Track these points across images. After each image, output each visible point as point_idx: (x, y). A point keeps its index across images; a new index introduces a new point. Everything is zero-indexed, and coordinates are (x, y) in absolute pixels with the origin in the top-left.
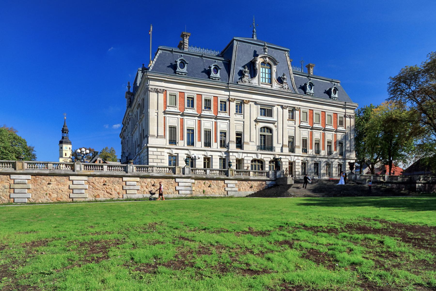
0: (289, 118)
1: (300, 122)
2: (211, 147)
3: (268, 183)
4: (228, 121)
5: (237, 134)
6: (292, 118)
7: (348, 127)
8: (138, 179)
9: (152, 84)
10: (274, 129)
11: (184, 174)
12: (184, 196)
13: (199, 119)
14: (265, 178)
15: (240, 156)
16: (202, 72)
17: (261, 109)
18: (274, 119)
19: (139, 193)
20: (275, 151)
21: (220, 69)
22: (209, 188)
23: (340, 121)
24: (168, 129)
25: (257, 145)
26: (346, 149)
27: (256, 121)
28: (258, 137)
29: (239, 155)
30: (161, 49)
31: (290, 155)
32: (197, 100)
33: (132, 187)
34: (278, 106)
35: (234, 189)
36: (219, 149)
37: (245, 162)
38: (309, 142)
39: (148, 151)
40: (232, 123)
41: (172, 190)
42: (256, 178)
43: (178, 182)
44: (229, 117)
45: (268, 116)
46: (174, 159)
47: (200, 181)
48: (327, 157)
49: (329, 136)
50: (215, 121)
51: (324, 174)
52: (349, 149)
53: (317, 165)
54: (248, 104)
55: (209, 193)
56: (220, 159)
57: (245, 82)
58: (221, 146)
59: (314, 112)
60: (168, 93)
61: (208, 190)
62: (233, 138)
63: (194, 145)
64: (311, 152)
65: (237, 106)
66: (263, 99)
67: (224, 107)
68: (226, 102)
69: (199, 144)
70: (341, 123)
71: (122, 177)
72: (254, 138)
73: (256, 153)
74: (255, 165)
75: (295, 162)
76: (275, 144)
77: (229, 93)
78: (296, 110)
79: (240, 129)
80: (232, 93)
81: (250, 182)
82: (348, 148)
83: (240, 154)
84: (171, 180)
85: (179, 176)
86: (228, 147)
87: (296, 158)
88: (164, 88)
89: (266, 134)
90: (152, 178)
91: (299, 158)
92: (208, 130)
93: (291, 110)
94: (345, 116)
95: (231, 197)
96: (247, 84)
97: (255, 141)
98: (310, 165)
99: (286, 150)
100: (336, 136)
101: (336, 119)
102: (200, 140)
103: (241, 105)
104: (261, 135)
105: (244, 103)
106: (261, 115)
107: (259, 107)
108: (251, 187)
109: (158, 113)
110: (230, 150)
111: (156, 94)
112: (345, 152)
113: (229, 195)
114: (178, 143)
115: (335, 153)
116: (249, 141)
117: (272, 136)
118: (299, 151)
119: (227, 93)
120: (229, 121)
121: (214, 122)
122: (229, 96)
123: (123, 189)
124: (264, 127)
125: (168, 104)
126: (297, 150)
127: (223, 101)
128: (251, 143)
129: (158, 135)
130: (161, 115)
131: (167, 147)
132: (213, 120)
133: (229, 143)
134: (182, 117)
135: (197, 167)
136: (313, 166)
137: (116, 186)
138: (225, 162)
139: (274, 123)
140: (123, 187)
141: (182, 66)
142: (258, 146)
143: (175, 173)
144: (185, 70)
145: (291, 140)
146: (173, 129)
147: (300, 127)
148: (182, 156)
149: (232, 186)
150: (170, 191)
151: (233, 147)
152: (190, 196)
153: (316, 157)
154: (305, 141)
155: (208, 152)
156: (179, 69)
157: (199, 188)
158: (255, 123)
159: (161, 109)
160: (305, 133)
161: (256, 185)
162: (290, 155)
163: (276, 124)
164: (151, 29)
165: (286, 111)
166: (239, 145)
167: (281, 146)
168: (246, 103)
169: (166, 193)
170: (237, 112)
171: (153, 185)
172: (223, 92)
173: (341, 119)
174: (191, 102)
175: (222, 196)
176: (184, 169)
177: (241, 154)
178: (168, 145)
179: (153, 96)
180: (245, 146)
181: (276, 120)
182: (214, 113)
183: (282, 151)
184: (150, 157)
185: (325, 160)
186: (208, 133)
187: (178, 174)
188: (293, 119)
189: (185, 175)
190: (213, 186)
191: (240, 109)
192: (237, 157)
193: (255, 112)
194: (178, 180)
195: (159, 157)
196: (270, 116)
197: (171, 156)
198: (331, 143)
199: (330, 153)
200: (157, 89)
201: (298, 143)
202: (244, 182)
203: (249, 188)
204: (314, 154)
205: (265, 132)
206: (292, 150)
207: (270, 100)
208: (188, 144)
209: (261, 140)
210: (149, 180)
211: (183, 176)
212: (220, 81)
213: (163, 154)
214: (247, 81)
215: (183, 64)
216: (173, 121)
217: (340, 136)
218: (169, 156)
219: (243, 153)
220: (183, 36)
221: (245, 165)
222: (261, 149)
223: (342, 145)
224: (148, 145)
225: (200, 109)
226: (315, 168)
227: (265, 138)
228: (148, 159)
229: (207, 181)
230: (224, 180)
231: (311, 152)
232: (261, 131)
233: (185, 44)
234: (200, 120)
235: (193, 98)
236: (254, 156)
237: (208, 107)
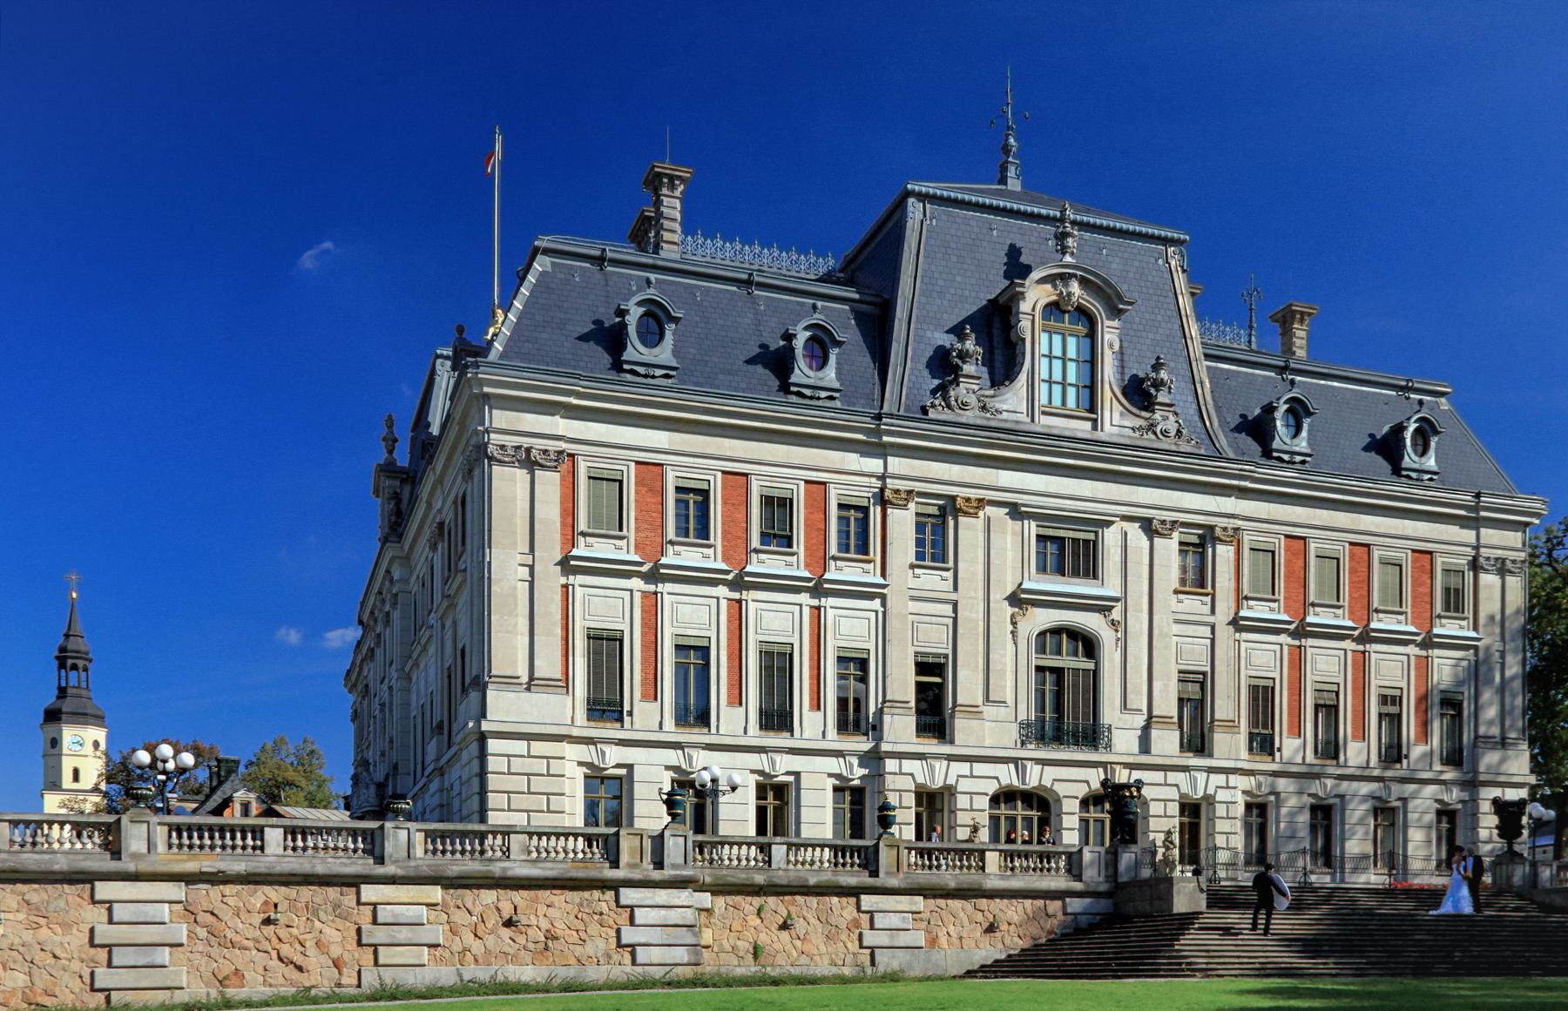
0: (1183, 582)
1: (1240, 599)
2: (791, 731)
3: (1075, 905)
4: (878, 601)
5: (923, 668)
6: (1198, 579)
7: (1492, 618)
8: (436, 893)
9: (506, 425)
10: (1107, 636)
11: (659, 864)
12: (657, 973)
13: (736, 596)
14: (1059, 882)
15: (940, 775)
16: (750, 362)
17: (1041, 538)
18: (1111, 588)
19: (439, 961)
20: (1109, 746)
21: (839, 344)
22: (785, 935)
23: (1447, 591)
24: (580, 644)
25: (1022, 716)
26: (1482, 730)
27: (1015, 599)
28: (1027, 680)
29: (932, 769)
30: (546, 252)
31: (1185, 769)
32: (724, 503)
33: (403, 934)
34: (1126, 525)
35: (904, 939)
36: (834, 740)
37: (962, 802)
38: (1282, 700)
39: (483, 755)
40: (896, 612)
41: (600, 943)
42: (1016, 883)
43: (632, 907)
44: (882, 581)
45: (1076, 573)
46: (610, 795)
47: (739, 898)
48: (1376, 773)
49: (1390, 669)
50: (815, 602)
51: (1365, 857)
52: (1495, 731)
53: (1324, 815)
54: (975, 516)
55: (781, 960)
56: (836, 789)
57: (964, 406)
58: (842, 726)
59: (1312, 546)
60: (582, 467)
61: (777, 946)
62: (904, 684)
63: (708, 725)
64: (1293, 748)
65: (920, 528)
66: (1052, 490)
67: (858, 533)
68: (865, 510)
69: (735, 719)
70: (1454, 602)
71: (354, 882)
72: (1005, 686)
73: (1015, 761)
74: (1012, 820)
75: (1210, 800)
76: (1110, 713)
77: (880, 462)
78: (1216, 540)
79: (936, 642)
80: (896, 464)
81: (983, 903)
82: (1490, 723)
83: (937, 764)
84: (596, 894)
85: (636, 875)
86: (876, 729)
87: (1219, 779)
88: (563, 445)
89: (1066, 662)
90: (505, 887)
91: (1234, 780)
92: (776, 649)
93: (1195, 540)
94: (1475, 565)
95: (893, 978)
96: (969, 416)
97: (1010, 700)
98: (1292, 815)
99: (1167, 743)
100: (1424, 665)
101: (1426, 578)
102: (738, 699)
103: (944, 523)
104: (1039, 669)
105: (957, 512)
106: (1042, 569)
107: (1032, 528)
108: (991, 929)
109: (532, 568)
110: (885, 747)
111: (521, 475)
112: (1475, 745)
113: (881, 969)
114: (630, 713)
115: (1417, 751)
116: (980, 700)
117: (1096, 673)
118: (1231, 746)
119: (875, 465)
120: (884, 604)
121: (806, 610)
122: (883, 478)
123: (360, 944)
124: (1057, 631)
125: (582, 526)
126: (1220, 740)
127: (854, 502)
128: (989, 711)
129: (531, 678)
130: (551, 579)
131: (575, 732)
132: (804, 598)
133: (880, 713)
134: (652, 588)
135: (725, 829)
136: (1304, 818)
137: (327, 930)
138: (861, 805)
139: (1104, 610)
140: (359, 931)
141: (652, 336)
142: (1024, 725)
143: (615, 864)
144: (664, 353)
145: (1193, 690)
146: (605, 646)
147: (1236, 623)
148: (652, 776)
149: (894, 921)
150: (590, 949)
151: (901, 729)
152: (688, 972)
153: (1317, 776)
154: (1262, 698)
155: (778, 757)
156: (636, 351)
157: (735, 933)
158: (1010, 610)
159: (550, 550)
160: (1265, 657)
161: (1016, 918)
162: (1185, 769)
163: (1116, 614)
164: (498, 147)
165: (1169, 548)
166: (928, 719)
167: (1140, 720)
168: (967, 514)
169: (573, 961)
170: (920, 556)
171: (509, 923)
172: (853, 461)
173: (1454, 582)
174: (695, 512)
175: (847, 971)
176: (658, 840)
177: (941, 766)
178: (581, 725)
179: (508, 484)
180: (963, 727)
181: (1116, 593)
182: (807, 566)
183: (1145, 746)
184: (493, 782)
185: (1365, 788)
186: (777, 664)
187: (631, 866)
188: (1202, 586)
189: (668, 873)
190: (800, 926)
191: (935, 544)
192: (920, 780)
193: (1010, 554)
194: (629, 896)
195: (539, 784)
196: (1086, 575)
197: (595, 777)
198: (1396, 700)
199: (1393, 753)
200: (528, 450)
201: (1229, 704)
202: (956, 904)
203: (978, 932)
204: (1310, 757)
205: (1059, 653)
206: (1197, 742)
207: (1088, 494)
208: (682, 719)
209: (1041, 694)
210: (489, 896)
211: (657, 875)
212: (838, 404)
213: (556, 767)
214: (972, 400)
215: (656, 320)
216: (606, 605)
217: (1445, 668)
218: (586, 777)
219: (951, 758)
220: (654, 182)
221: (963, 818)
222: (1041, 739)
223: (1460, 714)
224: (485, 726)
225: (738, 548)
226: (1313, 828)
227: (1059, 682)
228: (483, 792)
229: (772, 900)
230: (855, 892)
231: (1293, 748)
232: (1041, 649)
233: (667, 224)
234: (739, 602)
235: (705, 493)
236: (1007, 776)
237: (778, 536)
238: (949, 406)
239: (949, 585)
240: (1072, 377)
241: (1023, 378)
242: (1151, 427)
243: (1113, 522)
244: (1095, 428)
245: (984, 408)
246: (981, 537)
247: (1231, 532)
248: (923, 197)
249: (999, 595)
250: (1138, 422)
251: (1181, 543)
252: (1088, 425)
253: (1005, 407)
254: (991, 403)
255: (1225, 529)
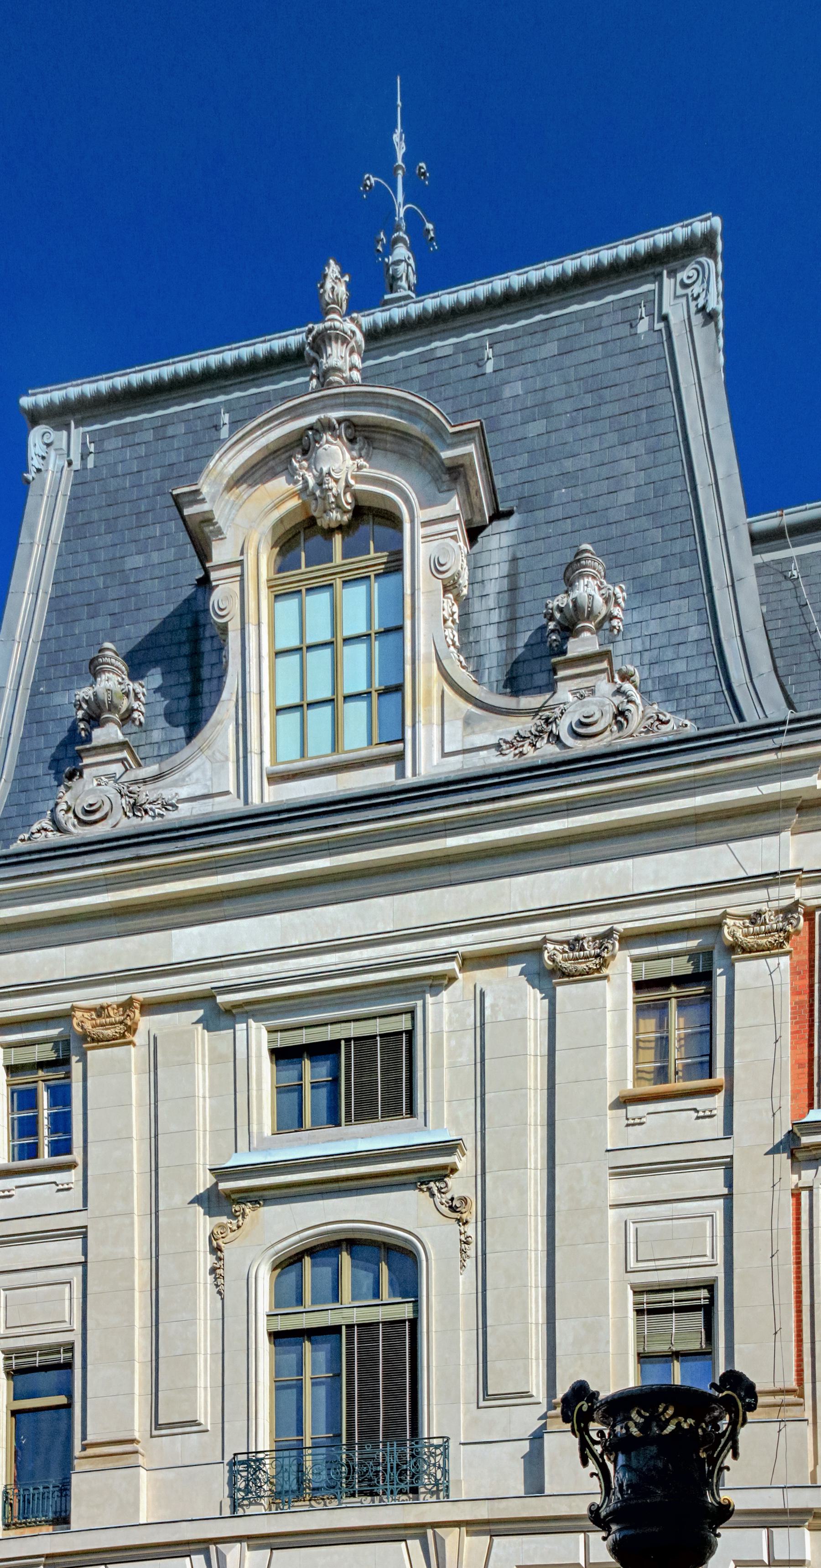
0: (662, 1074)
17: (279, 1055)
27: (214, 1201)
34: (482, 976)
45: (365, 1112)
103: (68, 1076)
106: (290, 1120)
107: (258, 1037)
139: (431, 1179)
167: (527, 1419)
168: (100, 1042)
232: (288, 1296)
238: (58, 827)
239: (74, 1200)
240: (355, 678)
241: (224, 714)
242: (546, 730)
243: (453, 979)
244: (401, 774)
245: (135, 806)
246: (137, 1084)
247: (773, 921)
248: (59, 415)
249: (175, 1198)
250: (510, 728)
251: (639, 986)
252: (391, 769)
253: (184, 793)
254: (146, 793)
255: (755, 918)
